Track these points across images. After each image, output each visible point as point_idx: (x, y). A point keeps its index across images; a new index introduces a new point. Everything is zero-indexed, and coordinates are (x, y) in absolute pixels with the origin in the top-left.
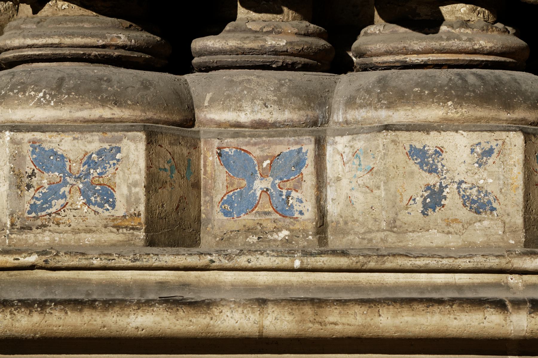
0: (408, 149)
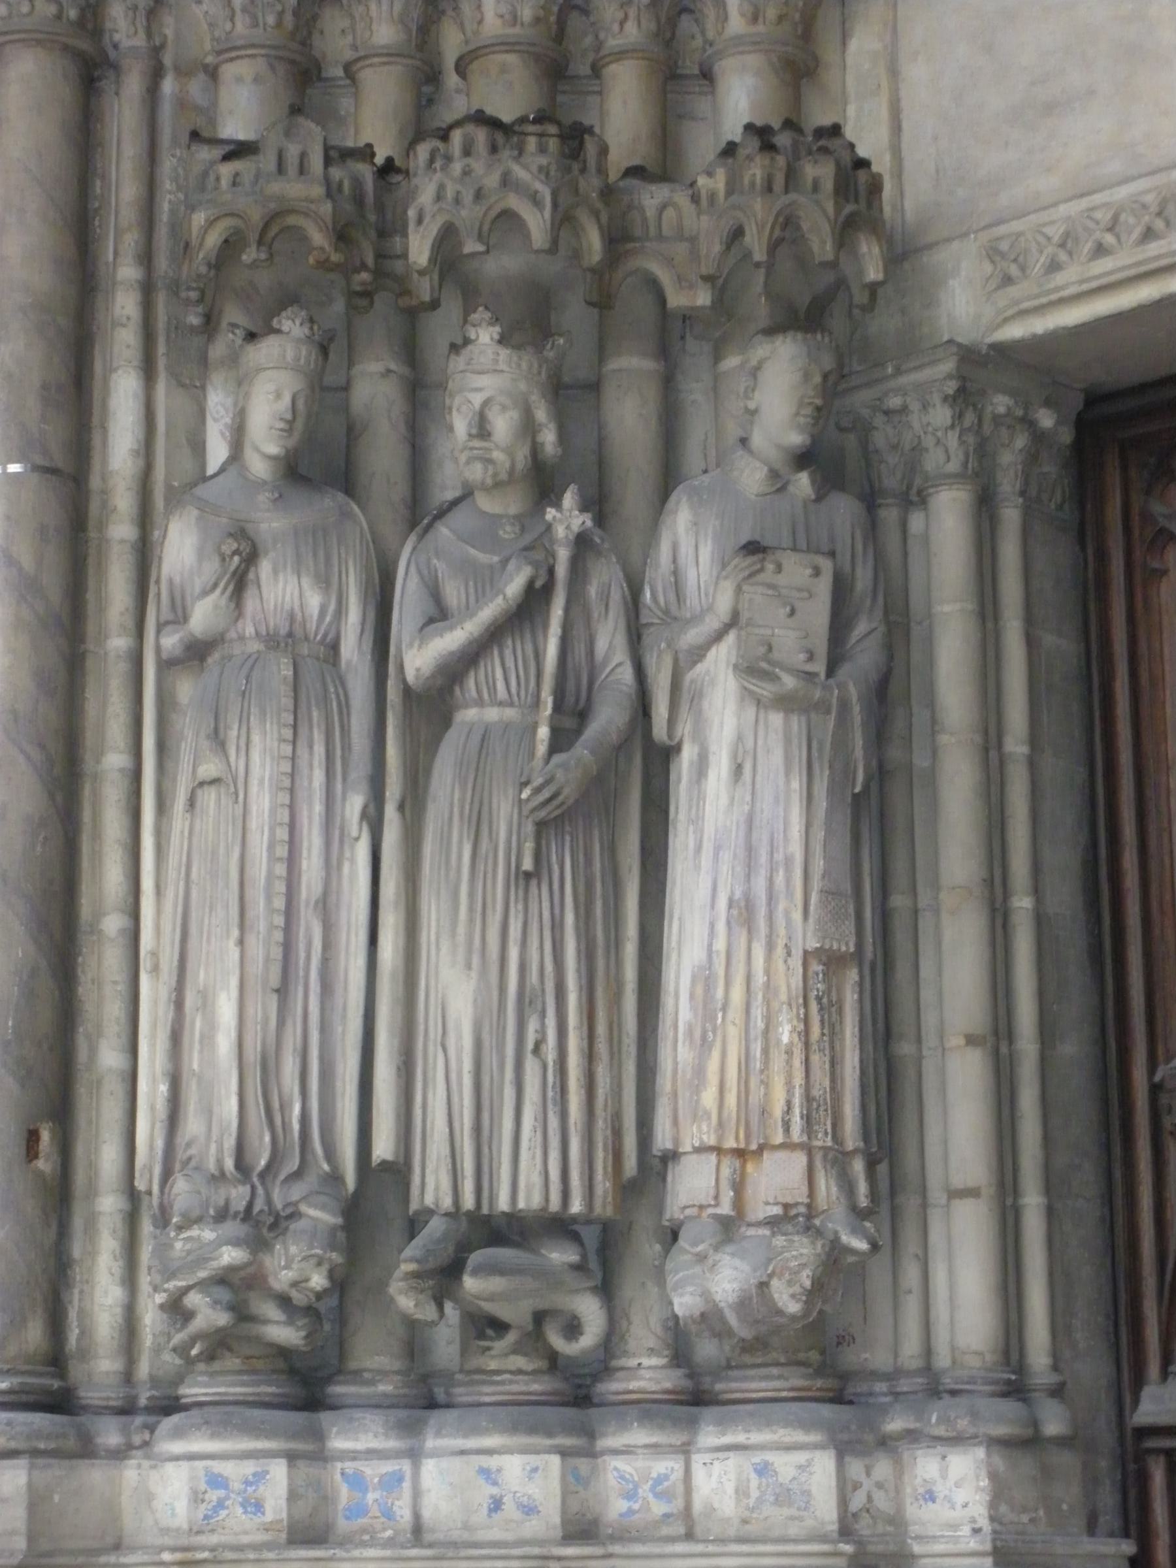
0: (477, 1468)
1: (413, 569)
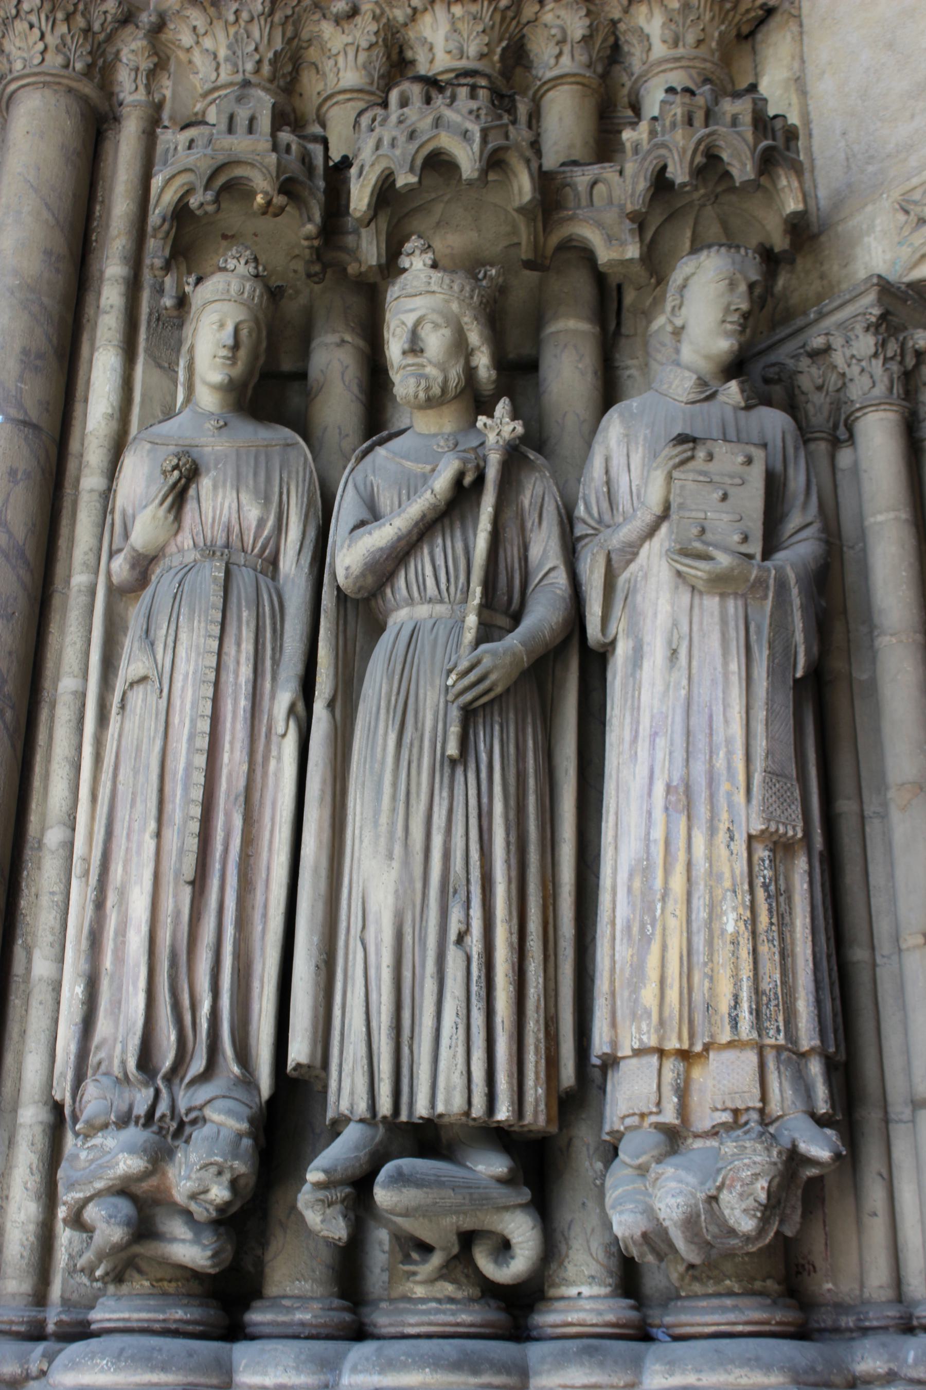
1: (350, 485)
